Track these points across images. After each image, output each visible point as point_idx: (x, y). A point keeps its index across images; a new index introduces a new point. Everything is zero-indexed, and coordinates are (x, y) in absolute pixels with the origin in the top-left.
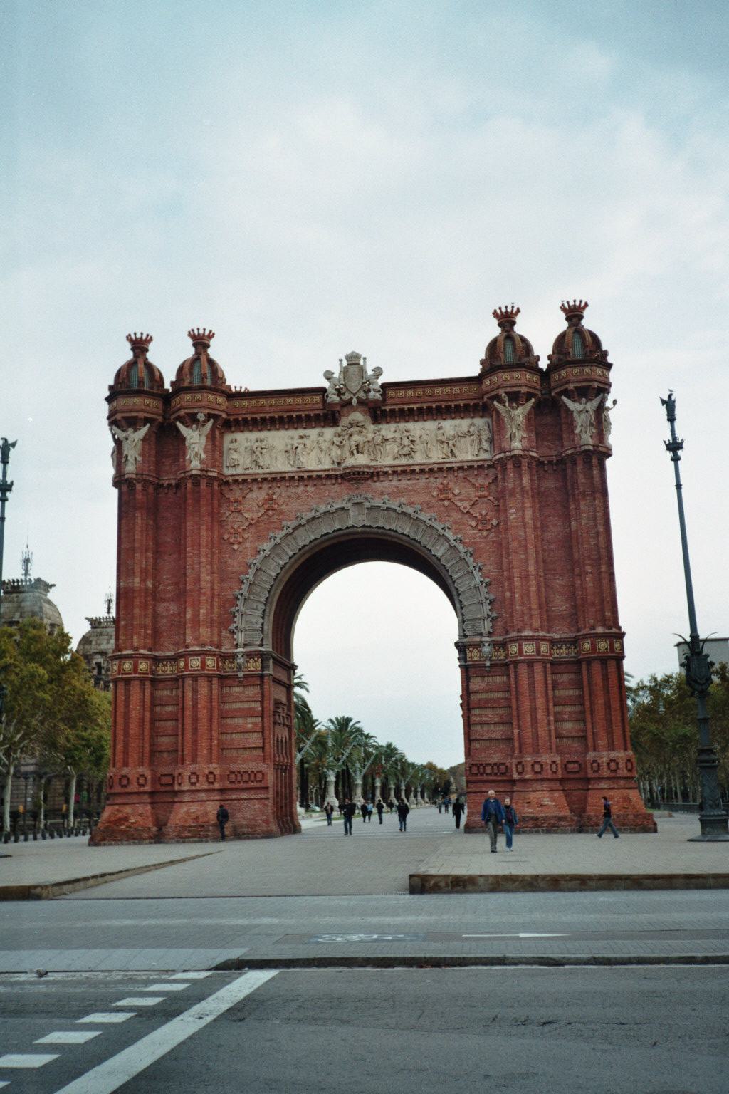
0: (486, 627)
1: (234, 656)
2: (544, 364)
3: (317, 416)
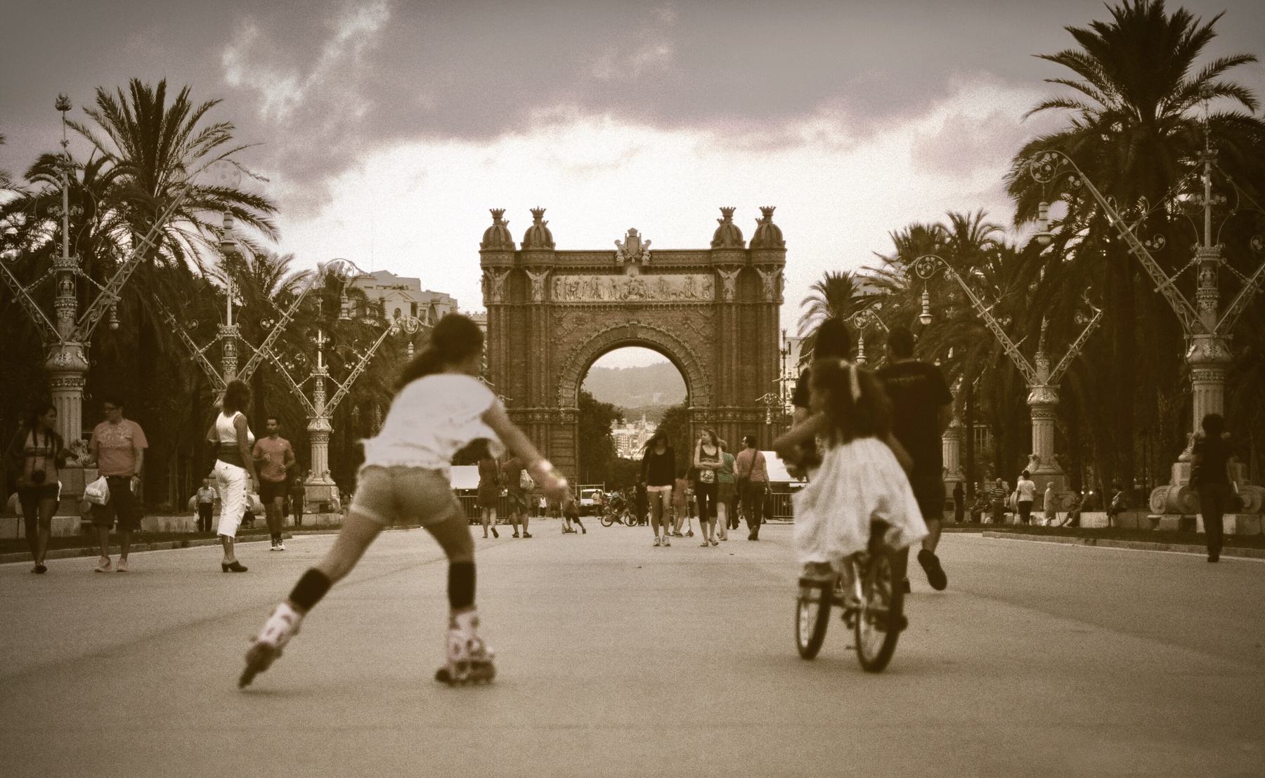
0: (707, 401)
1: (558, 413)
2: (747, 246)
3: (610, 268)
